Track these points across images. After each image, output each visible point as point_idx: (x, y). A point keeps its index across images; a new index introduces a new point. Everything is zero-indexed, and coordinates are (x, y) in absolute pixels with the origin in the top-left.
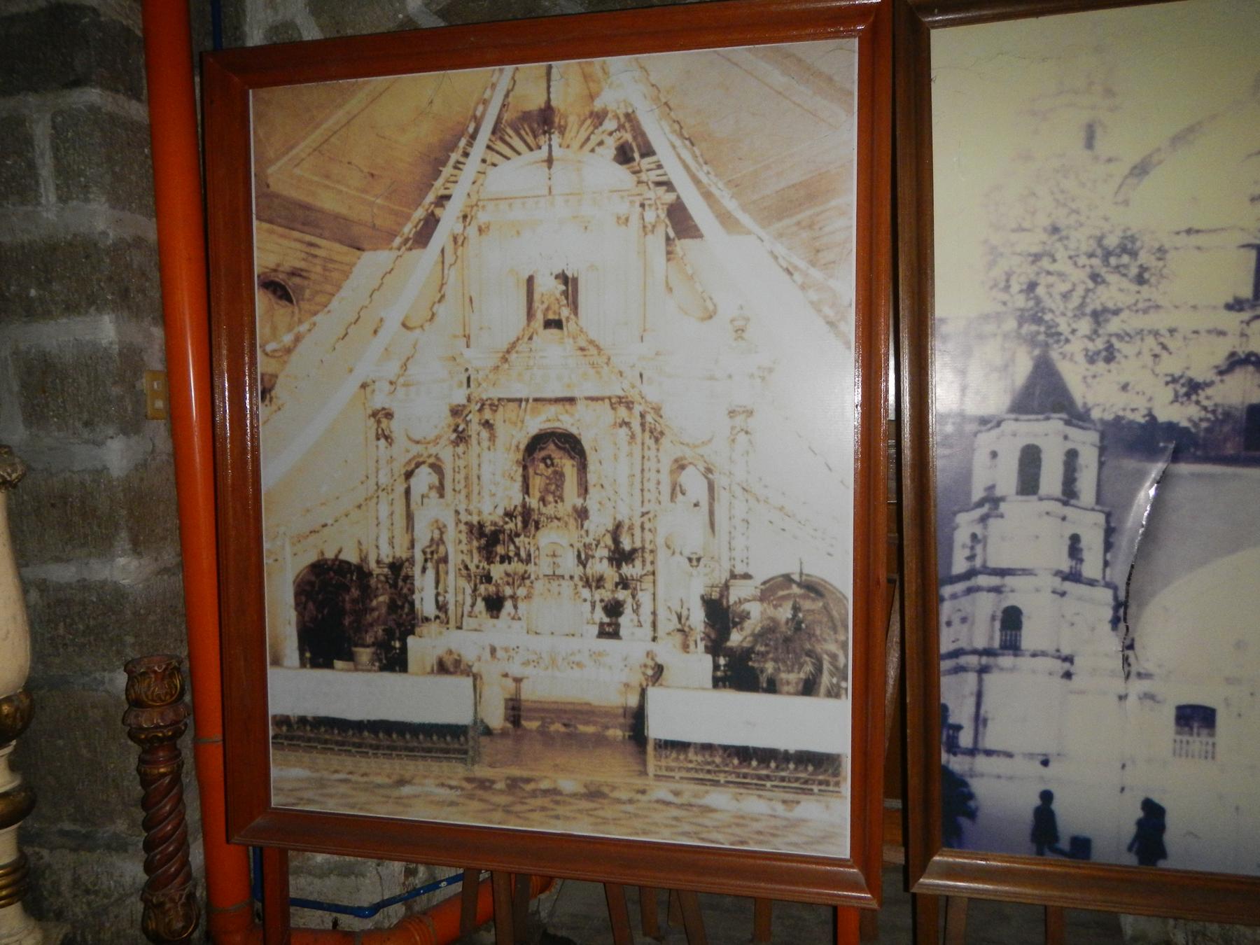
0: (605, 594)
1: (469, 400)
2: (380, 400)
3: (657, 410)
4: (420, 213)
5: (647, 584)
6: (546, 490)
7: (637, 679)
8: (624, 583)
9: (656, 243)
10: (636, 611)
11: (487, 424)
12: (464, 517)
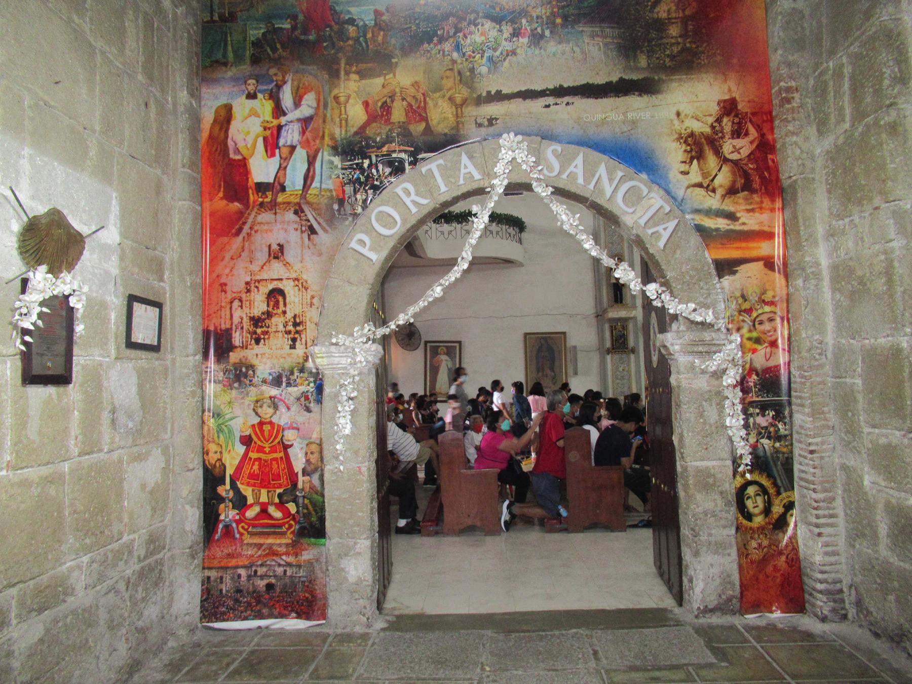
2: (223, 280)
4: (237, 227)
6: (274, 306)
7: (301, 360)
8: (297, 332)
9: (305, 236)
11: (257, 287)
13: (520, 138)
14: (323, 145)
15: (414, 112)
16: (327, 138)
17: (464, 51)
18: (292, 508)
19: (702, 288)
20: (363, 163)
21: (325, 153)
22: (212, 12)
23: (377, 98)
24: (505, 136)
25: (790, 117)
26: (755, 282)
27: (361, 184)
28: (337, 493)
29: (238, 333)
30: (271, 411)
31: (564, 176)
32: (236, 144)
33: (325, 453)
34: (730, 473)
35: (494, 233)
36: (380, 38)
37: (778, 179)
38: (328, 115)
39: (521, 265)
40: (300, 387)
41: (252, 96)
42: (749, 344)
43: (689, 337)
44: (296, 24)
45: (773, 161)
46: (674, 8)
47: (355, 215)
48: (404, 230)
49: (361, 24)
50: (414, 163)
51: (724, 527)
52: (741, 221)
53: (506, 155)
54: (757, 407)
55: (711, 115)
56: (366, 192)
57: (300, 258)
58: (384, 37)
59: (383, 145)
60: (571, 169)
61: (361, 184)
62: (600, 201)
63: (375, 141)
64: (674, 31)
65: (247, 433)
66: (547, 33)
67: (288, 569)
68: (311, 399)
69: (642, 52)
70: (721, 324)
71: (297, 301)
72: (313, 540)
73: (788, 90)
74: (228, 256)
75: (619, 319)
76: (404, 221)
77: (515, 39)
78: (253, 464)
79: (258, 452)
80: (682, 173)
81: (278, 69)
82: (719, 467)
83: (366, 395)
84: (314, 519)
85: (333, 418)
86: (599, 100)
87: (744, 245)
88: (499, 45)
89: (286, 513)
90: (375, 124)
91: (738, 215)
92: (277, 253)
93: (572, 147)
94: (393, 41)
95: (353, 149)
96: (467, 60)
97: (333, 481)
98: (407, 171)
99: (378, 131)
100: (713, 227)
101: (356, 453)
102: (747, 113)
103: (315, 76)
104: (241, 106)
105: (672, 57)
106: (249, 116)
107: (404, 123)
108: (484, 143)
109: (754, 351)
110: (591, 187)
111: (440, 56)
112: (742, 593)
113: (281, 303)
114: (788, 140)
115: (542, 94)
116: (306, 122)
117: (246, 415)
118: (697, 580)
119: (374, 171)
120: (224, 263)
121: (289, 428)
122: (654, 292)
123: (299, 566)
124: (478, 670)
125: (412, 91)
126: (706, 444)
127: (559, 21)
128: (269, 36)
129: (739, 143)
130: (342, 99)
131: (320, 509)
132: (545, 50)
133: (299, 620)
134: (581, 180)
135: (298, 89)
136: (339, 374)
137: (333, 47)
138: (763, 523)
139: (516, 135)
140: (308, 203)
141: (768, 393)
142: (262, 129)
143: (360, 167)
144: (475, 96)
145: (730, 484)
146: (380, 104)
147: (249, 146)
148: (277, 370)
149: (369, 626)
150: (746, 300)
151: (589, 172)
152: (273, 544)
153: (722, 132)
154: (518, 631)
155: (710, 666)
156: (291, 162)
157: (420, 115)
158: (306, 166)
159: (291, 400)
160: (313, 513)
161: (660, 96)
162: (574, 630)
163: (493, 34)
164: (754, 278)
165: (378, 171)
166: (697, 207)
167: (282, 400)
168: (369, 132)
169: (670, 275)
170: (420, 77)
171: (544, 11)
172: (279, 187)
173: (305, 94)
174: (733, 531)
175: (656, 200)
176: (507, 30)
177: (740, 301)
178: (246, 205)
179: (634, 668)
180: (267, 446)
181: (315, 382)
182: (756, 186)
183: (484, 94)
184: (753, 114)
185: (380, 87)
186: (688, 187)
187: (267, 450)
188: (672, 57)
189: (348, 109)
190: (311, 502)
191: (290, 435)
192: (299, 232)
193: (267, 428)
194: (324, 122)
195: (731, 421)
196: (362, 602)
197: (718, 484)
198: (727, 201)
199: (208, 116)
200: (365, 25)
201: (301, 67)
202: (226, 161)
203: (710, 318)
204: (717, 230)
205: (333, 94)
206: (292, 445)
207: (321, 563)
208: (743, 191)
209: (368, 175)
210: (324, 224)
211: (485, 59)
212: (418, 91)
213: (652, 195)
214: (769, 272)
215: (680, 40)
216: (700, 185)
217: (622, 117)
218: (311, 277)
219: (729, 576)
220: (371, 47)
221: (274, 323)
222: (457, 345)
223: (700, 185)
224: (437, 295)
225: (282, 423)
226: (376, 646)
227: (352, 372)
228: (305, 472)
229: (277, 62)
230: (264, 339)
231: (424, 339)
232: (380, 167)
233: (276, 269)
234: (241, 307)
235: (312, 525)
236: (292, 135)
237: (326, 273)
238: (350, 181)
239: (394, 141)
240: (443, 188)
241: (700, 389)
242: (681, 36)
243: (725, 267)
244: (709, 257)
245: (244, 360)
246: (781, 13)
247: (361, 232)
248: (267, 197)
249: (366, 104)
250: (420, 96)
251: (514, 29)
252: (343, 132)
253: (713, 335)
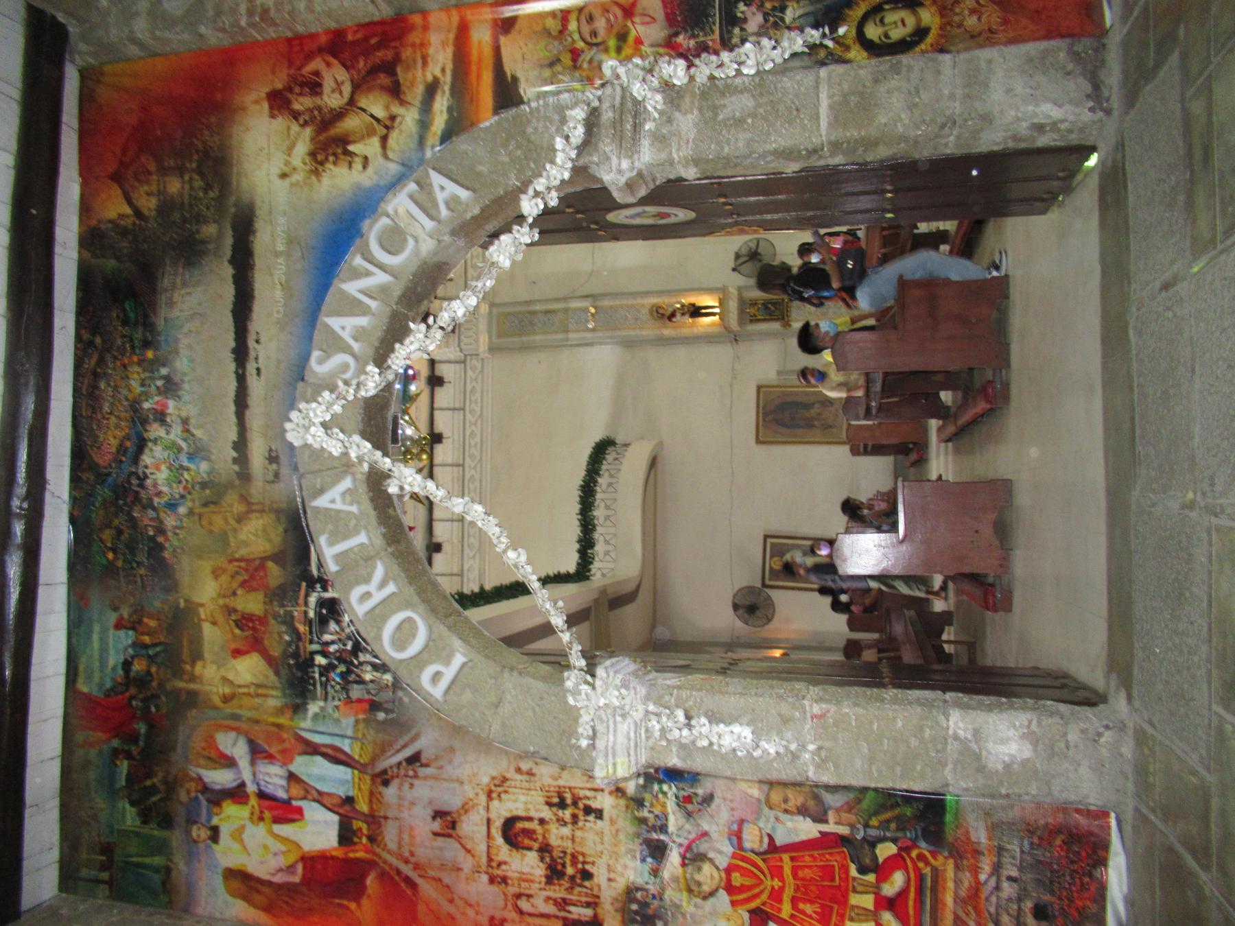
0: (581, 814)
1: (487, 873)
3: (493, 778)
4: (403, 885)
5: (576, 791)
6: (531, 839)
7: (622, 802)
8: (575, 803)
9: (423, 771)
10: (588, 798)
11: (500, 864)
12: (542, 885)
13: (294, 415)
14: (291, 727)
15: (252, 577)
16: (281, 721)
17: (177, 496)
18: (886, 850)
19: (536, 129)
20: (320, 666)
21: (303, 725)
22: (98, 881)
23: (230, 636)
24: (290, 437)
25: (287, 7)
26: (530, 46)
27: (349, 672)
28: (858, 763)
29: (572, 908)
30: (707, 868)
31: (356, 346)
32: (281, 870)
33: (784, 777)
34: (839, 69)
35: (613, 480)
36: (153, 623)
37: (382, 23)
38: (248, 714)
39: (660, 445)
40: (669, 810)
41: (215, 834)
42: (627, 51)
43: (607, 145)
44: (123, 751)
45: (355, 32)
46: (146, 188)
47: (396, 685)
48: (421, 608)
49: (131, 651)
50: (325, 584)
51: (939, 72)
52: (438, 72)
53: (317, 437)
54: (730, 32)
55: (289, 128)
56: (361, 664)
57: (457, 785)
58: (150, 616)
59: (295, 631)
60: (346, 336)
61: (349, 672)
62: (397, 292)
63: (289, 644)
64: (174, 186)
65: (746, 916)
66: (164, 371)
67: (1005, 873)
68: (689, 791)
69: (198, 231)
70: (591, 94)
71: (523, 798)
72: (948, 818)
73: (250, 13)
74: (447, 907)
75: (741, 311)
76: (408, 605)
77: (168, 420)
78: (803, 913)
79: (780, 901)
80: (364, 167)
81: (181, 786)
82: (830, 86)
83: (684, 694)
84: (908, 812)
85: (724, 757)
86: (256, 293)
87: (474, 68)
88: (174, 443)
89: (895, 862)
90: (266, 642)
91: (430, 78)
92: (447, 821)
93: (317, 336)
94: (157, 604)
95: (299, 680)
96: (190, 493)
97: (836, 766)
98: (335, 595)
99: (277, 638)
100: (445, 116)
101: (785, 721)
102: (288, 75)
103: (194, 728)
104: (227, 854)
105: (208, 187)
106: (241, 842)
107: (266, 596)
108: (302, 470)
109: (639, 41)
110: (373, 304)
111: (182, 534)
112: (1062, 36)
113: (527, 825)
114: (318, 8)
115: (241, 379)
116: (257, 752)
117: (714, 913)
118: (1035, 115)
119: (332, 648)
120: (458, 917)
121: (740, 838)
122: (534, 201)
123: (1000, 850)
124: (1193, 514)
125: (224, 579)
126: (791, 112)
127: (150, 354)
128: (136, 796)
129: (328, 84)
130: (227, 690)
131: (888, 799)
132: (185, 374)
133: (1111, 863)
134: (363, 321)
135: (209, 758)
136: (648, 738)
137: (158, 697)
138: (933, 9)
139: (290, 420)
140: (375, 759)
141: (707, 16)
142: (262, 824)
143: (325, 670)
144: (237, 482)
145: (860, 67)
146: (237, 631)
147: (283, 848)
148: (637, 847)
149: (1122, 727)
150: (559, 60)
151: (353, 307)
152: (956, 894)
153: (310, 110)
154: (1133, 438)
155: (1184, 57)
156: (312, 784)
157: (256, 569)
158: (319, 759)
159: (690, 830)
160: (897, 811)
161: (258, 204)
162: (1131, 332)
163: (158, 451)
164: (524, 49)
165: (333, 642)
166: (416, 142)
167: (689, 848)
168: (276, 652)
169: (514, 181)
170: (206, 566)
171: (136, 376)
172: (347, 808)
173: (218, 749)
174: (947, 58)
175: (401, 203)
176: (156, 430)
177: (559, 68)
178: (372, 864)
179: (1190, 206)
180: (772, 883)
181: (660, 782)
182: (388, 54)
183: (236, 468)
184: (290, 66)
185: (216, 628)
186: (386, 157)
187: (777, 883)
188: (208, 187)
189: (242, 682)
190: (876, 813)
191: (752, 839)
192: (416, 782)
193: (737, 879)
194: (257, 722)
195: (751, 67)
196: (1073, 737)
197: (860, 88)
198: (409, 98)
199: (238, 908)
200: (134, 645)
201: (179, 750)
202: (304, 889)
203: (579, 113)
204: (450, 110)
205: (221, 704)
206: (770, 837)
207: (992, 807)
208: (395, 74)
209: (338, 659)
210: (406, 738)
211: (192, 466)
212: (224, 570)
213: (390, 209)
214: (517, 27)
215: (187, 178)
216: (384, 140)
217: (281, 260)
218: (485, 770)
219: (1030, 60)
220: (162, 639)
221: (559, 842)
222: (769, 541)
223: (384, 140)
224: (523, 558)
225: (729, 849)
226: (1155, 720)
227: (638, 715)
228: (821, 819)
229: (172, 786)
230: (584, 863)
231: (759, 585)
232: (327, 637)
233: (472, 826)
234: (529, 896)
235: (920, 816)
236: (273, 777)
237: (484, 745)
238: (345, 689)
239: (291, 612)
240: (362, 538)
241: (696, 125)
242: (182, 176)
243: (507, 94)
244: (489, 121)
245: (619, 905)
246: (152, 33)
247: (419, 677)
248: (360, 829)
249: (237, 653)
250: (232, 567)
251: (155, 420)
252: (273, 693)
253: (606, 105)
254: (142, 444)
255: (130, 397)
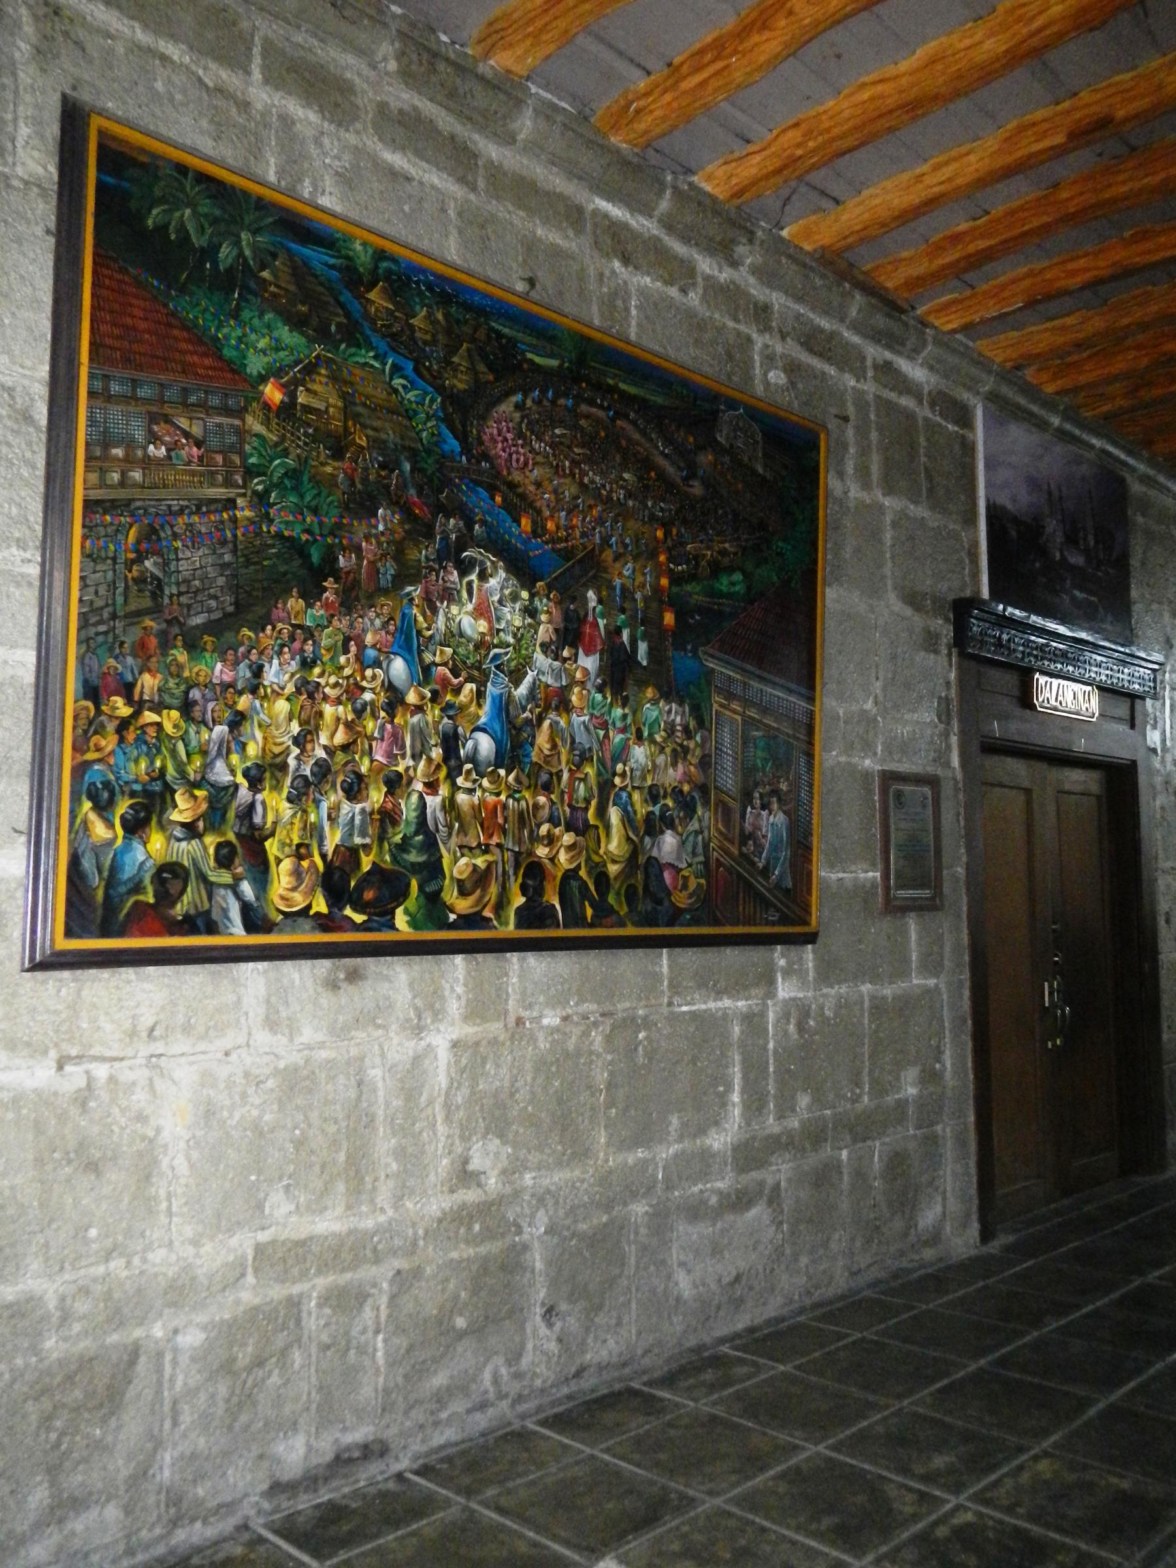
17: (428, 657)
96: (435, 697)
254: (524, 571)
255: (608, 555)
